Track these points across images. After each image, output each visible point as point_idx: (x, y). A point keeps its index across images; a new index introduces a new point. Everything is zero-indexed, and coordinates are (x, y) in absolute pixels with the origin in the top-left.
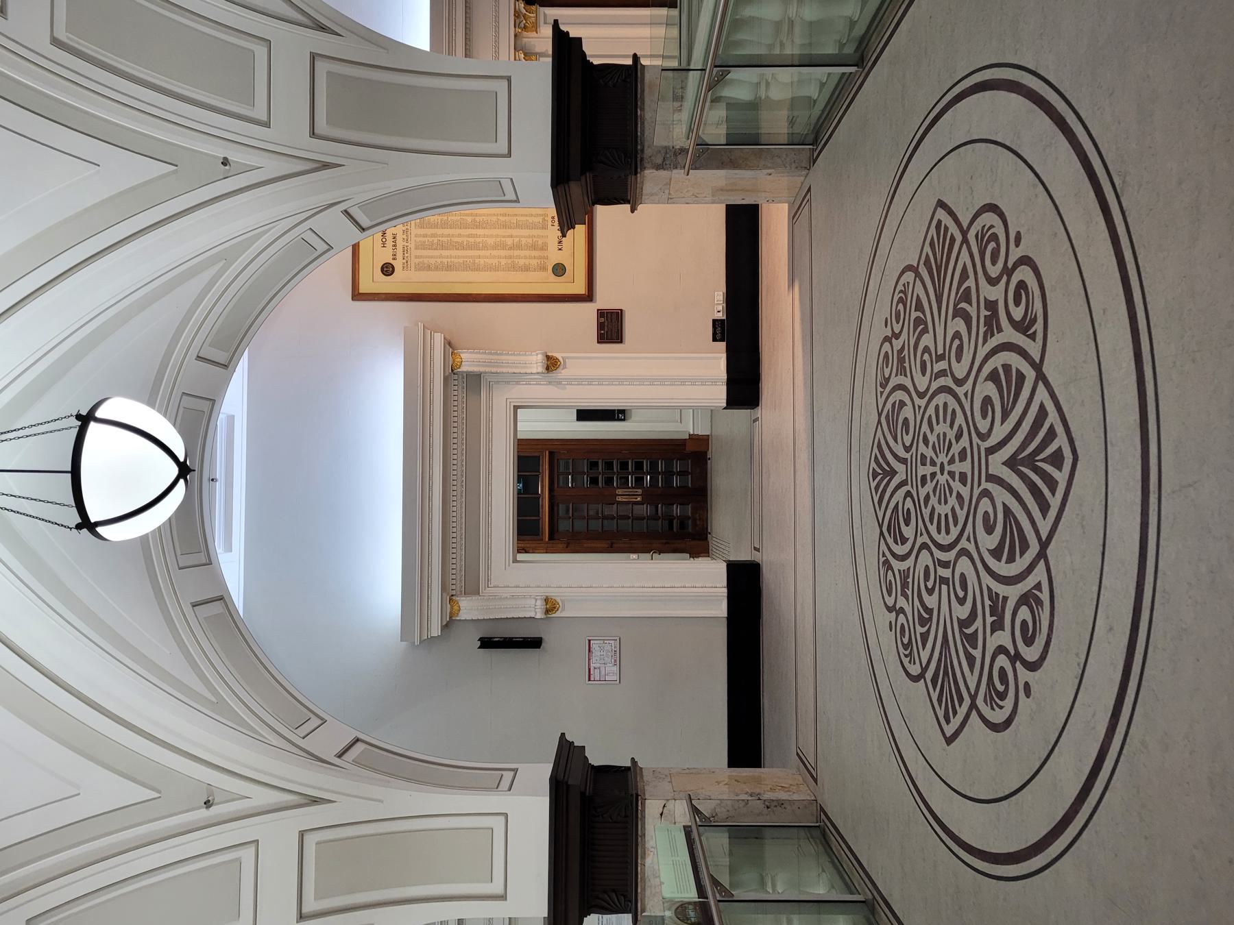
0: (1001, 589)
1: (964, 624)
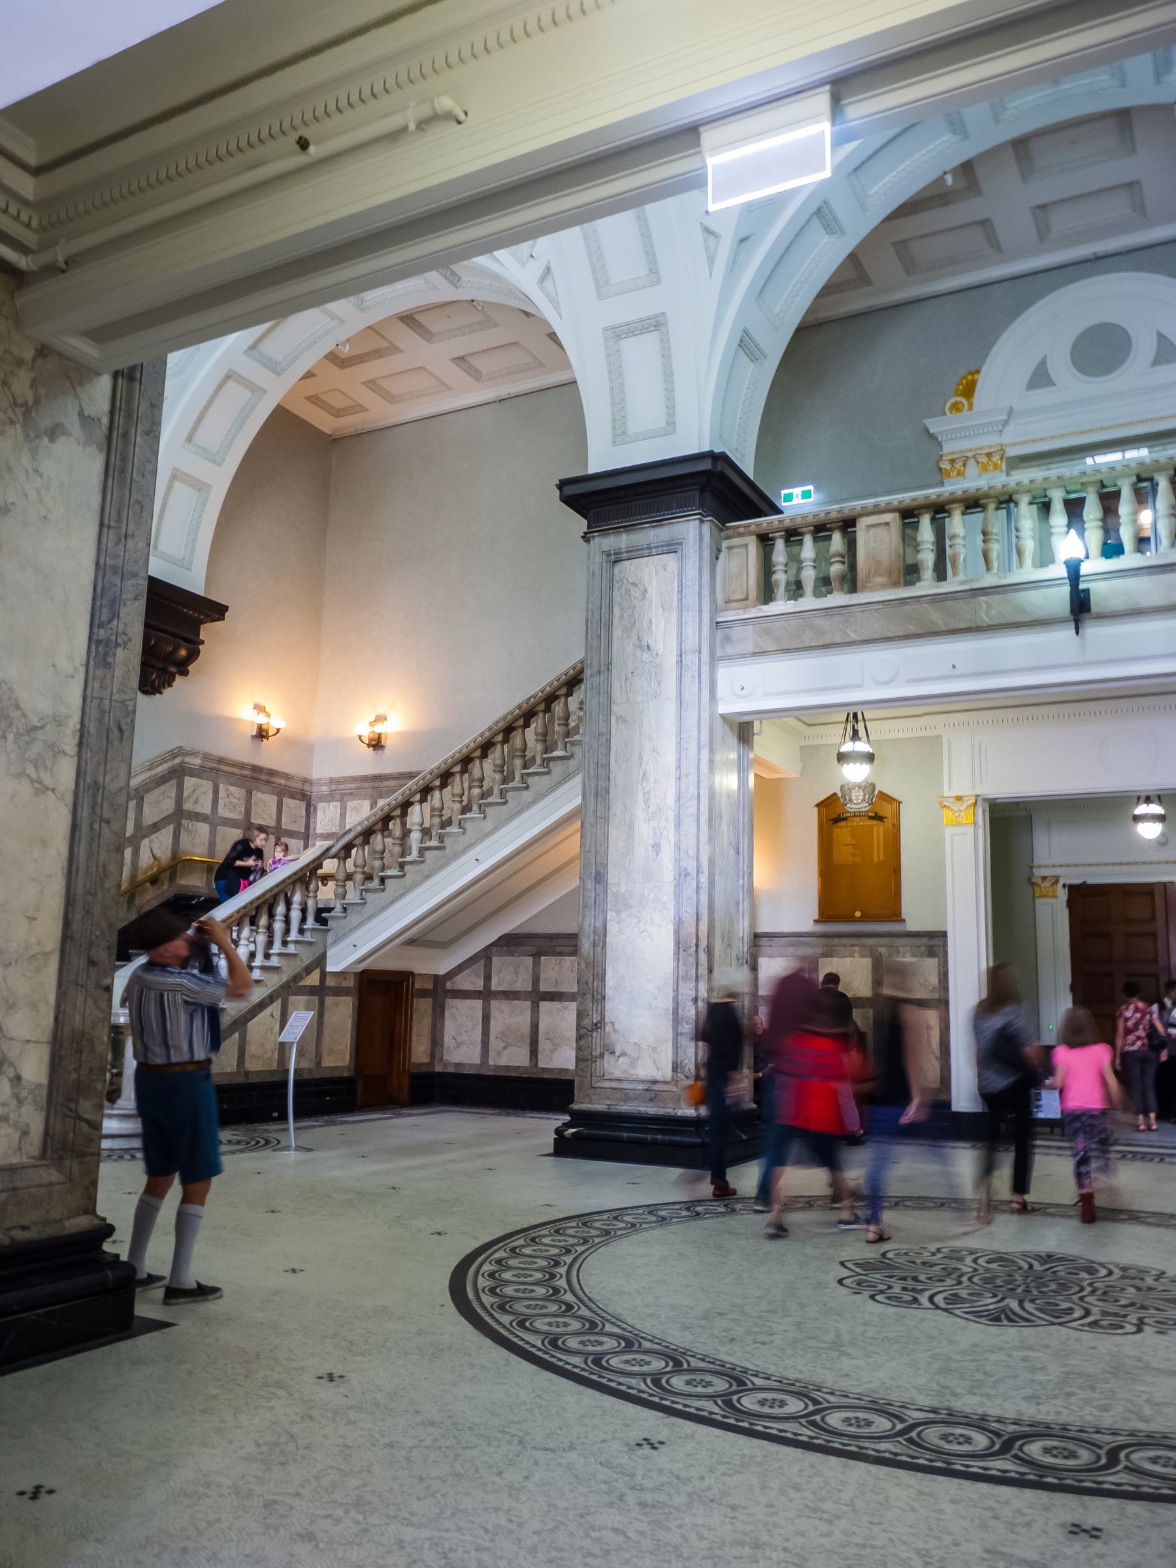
0: (927, 1294)
1: (915, 1279)
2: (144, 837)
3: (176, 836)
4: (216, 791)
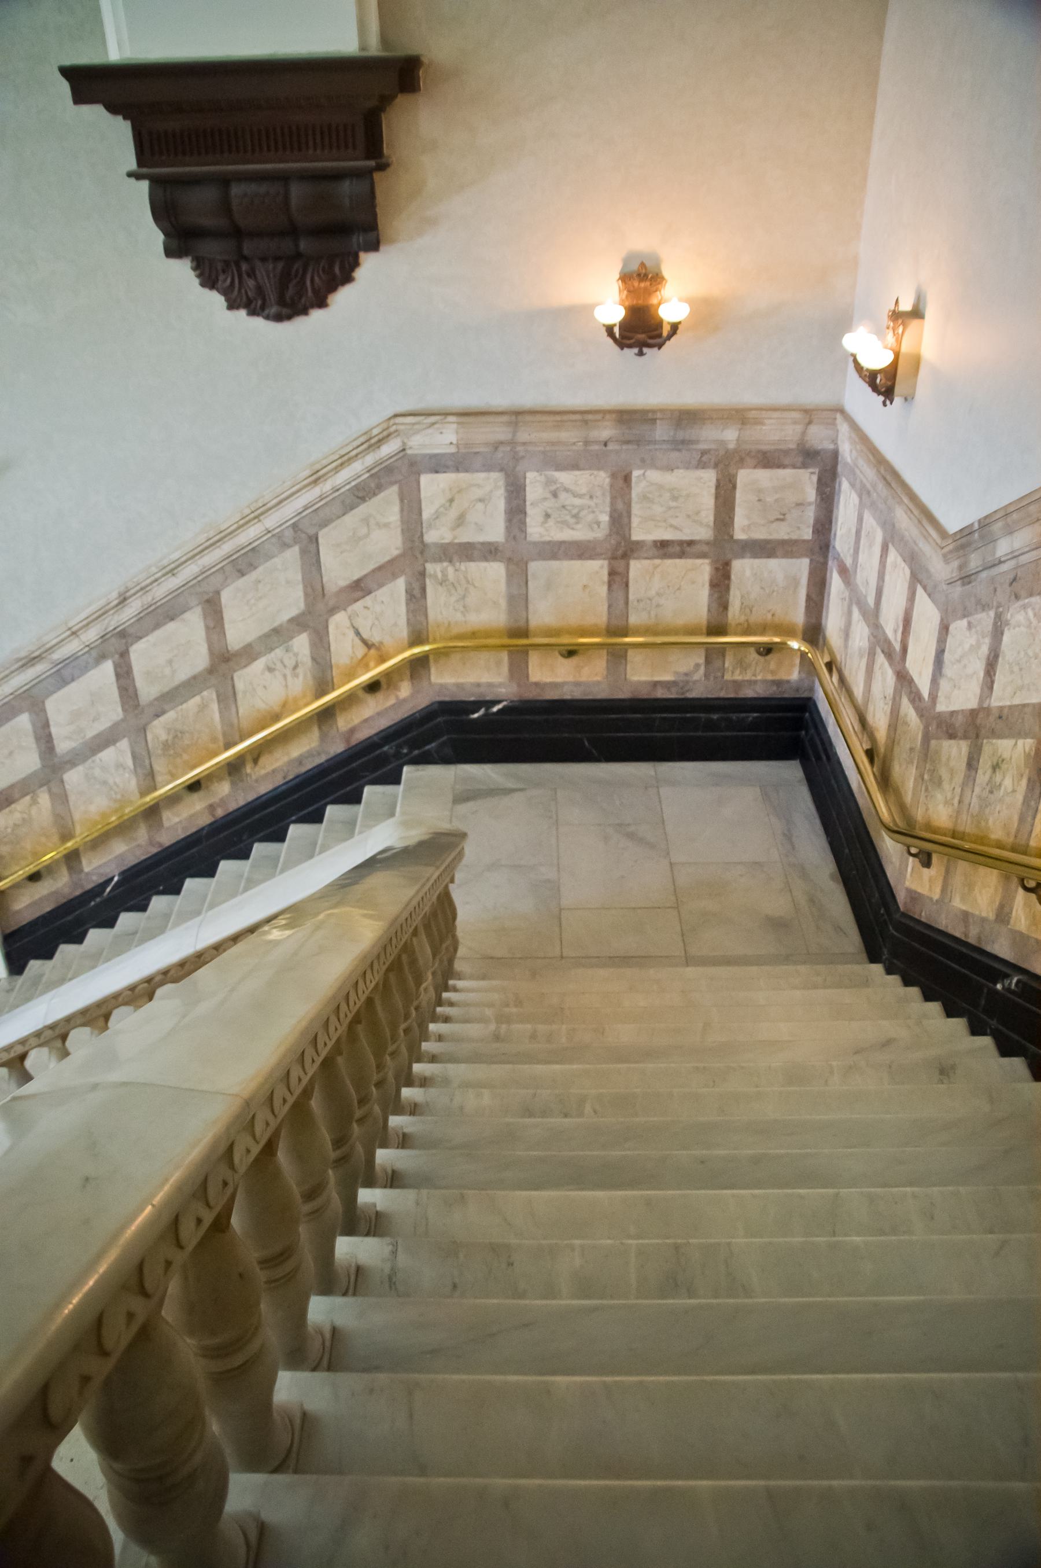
2: (332, 611)
3: (416, 597)
4: (516, 492)
